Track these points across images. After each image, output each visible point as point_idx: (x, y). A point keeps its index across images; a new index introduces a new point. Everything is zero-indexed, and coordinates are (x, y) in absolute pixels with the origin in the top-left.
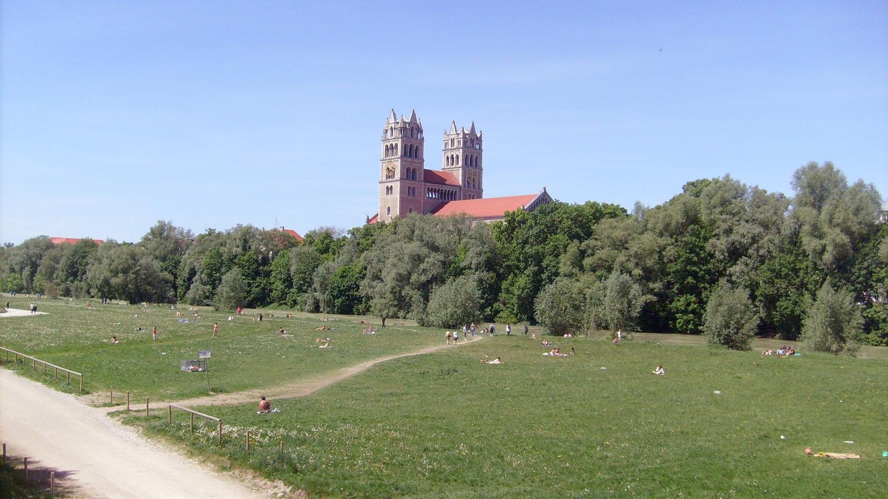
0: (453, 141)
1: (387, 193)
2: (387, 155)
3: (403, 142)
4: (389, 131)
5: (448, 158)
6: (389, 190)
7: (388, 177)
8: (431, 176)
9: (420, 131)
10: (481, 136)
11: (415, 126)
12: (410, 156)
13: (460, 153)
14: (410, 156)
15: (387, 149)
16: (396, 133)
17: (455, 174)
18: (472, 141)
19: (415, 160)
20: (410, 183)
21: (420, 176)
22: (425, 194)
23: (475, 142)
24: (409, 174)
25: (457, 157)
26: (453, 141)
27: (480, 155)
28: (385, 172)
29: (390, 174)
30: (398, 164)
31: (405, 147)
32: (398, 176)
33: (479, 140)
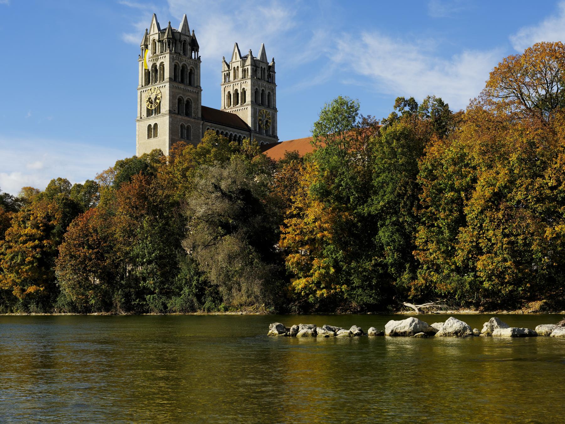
0: (236, 70)
1: (149, 137)
2: (148, 82)
3: (172, 60)
7: (149, 113)
9: (195, 46)
10: (273, 66)
11: (188, 39)
13: (248, 86)
17: (240, 115)
18: (263, 70)
19: (189, 88)
25: (244, 92)
27: (273, 91)
31: (174, 68)
32: (165, 107)
33: (271, 69)
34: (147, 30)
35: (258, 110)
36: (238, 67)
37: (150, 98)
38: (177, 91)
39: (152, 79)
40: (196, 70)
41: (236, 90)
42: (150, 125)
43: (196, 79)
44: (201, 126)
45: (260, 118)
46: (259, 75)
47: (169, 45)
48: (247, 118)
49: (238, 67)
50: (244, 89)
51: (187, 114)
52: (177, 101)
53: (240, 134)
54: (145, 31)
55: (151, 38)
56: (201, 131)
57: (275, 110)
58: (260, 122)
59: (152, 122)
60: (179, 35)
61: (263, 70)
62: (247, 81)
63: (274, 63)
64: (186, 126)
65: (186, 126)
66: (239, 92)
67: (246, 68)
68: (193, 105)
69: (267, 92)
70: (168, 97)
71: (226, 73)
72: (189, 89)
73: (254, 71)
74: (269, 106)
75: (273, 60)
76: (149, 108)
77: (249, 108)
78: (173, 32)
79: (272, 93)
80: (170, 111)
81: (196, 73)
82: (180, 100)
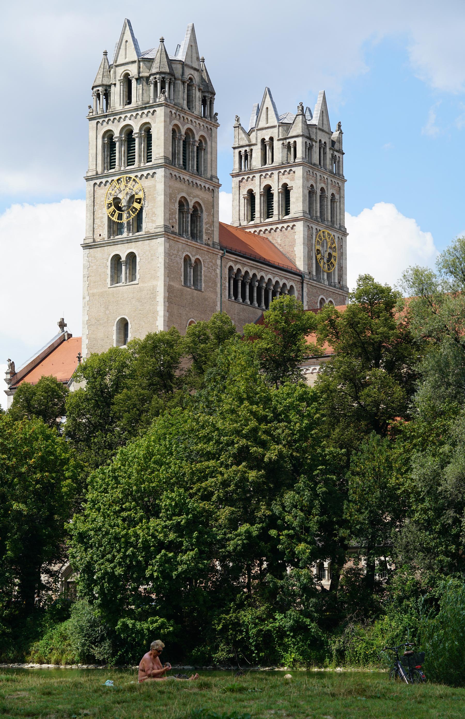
0: (267, 145)
2: (110, 162)
4: (117, 93)
5: (251, 196)
6: (123, 267)
7: (115, 228)
10: (340, 140)
15: (109, 144)
17: (277, 239)
20: (186, 247)
25: (286, 191)
26: (267, 145)
28: (104, 213)
29: (125, 217)
33: (336, 147)
34: (106, 53)
35: (314, 231)
36: (271, 139)
37: (117, 201)
38: (178, 185)
39: (120, 159)
40: (209, 143)
41: (268, 189)
42: (117, 258)
43: (209, 160)
44: (219, 262)
45: (318, 247)
47: (163, 87)
48: (293, 245)
49: (271, 139)
50: (285, 185)
51: (195, 236)
52: (177, 205)
53: (285, 281)
54: (103, 56)
55: (120, 71)
56: (218, 271)
57: (345, 234)
58: (319, 256)
59: (123, 251)
60: (179, 66)
61: (322, 147)
62: (293, 169)
63: (341, 133)
64: (193, 259)
65: (193, 259)
66: (275, 191)
67: (292, 141)
68: (205, 216)
70: (162, 197)
71: (243, 150)
72: (199, 183)
74: (332, 226)
75: (339, 126)
76: (115, 219)
77: (300, 226)
79: (337, 197)
80: (166, 227)
81: (209, 150)
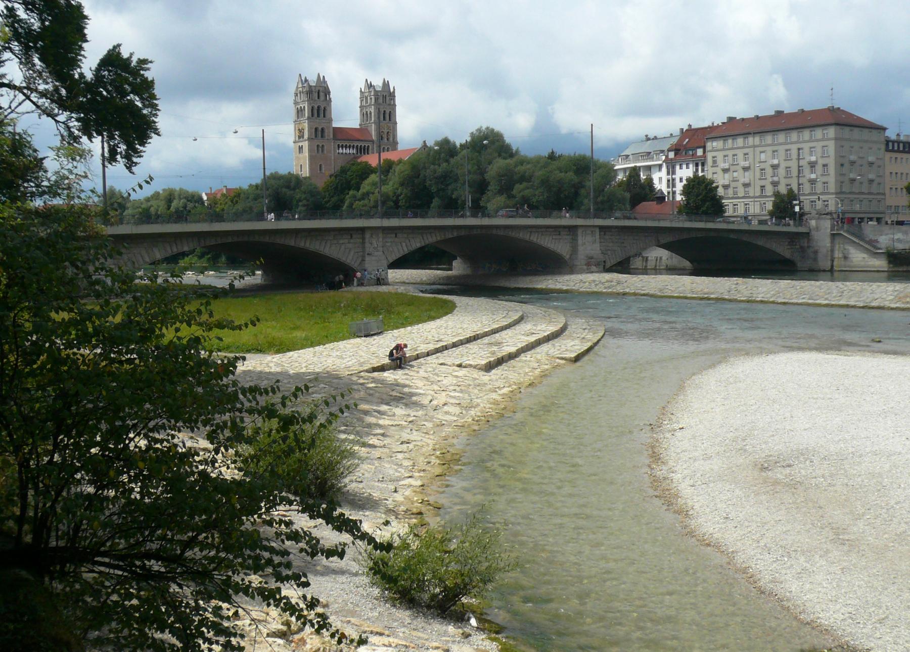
0: (366, 98)
7: (299, 137)
8: (341, 134)
11: (321, 89)
12: (318, 116)
13: (372, 109)
14: (318, 116)
15: (298, 112)
16: (304, 97)
18: (384, 97)
20: (319, 142)
21: (329, 134)
22: (335, 151)
23: (388, 98)
24: (318, 133)
30: (306, 125)
32: (306, 136)
33: (392, 95)
46: (381, 101)
59: (301, 144)
61: (384, 97)
69: (388, 112)
73: (376, 100)
78: (310, 87)
82: (316, 129)
